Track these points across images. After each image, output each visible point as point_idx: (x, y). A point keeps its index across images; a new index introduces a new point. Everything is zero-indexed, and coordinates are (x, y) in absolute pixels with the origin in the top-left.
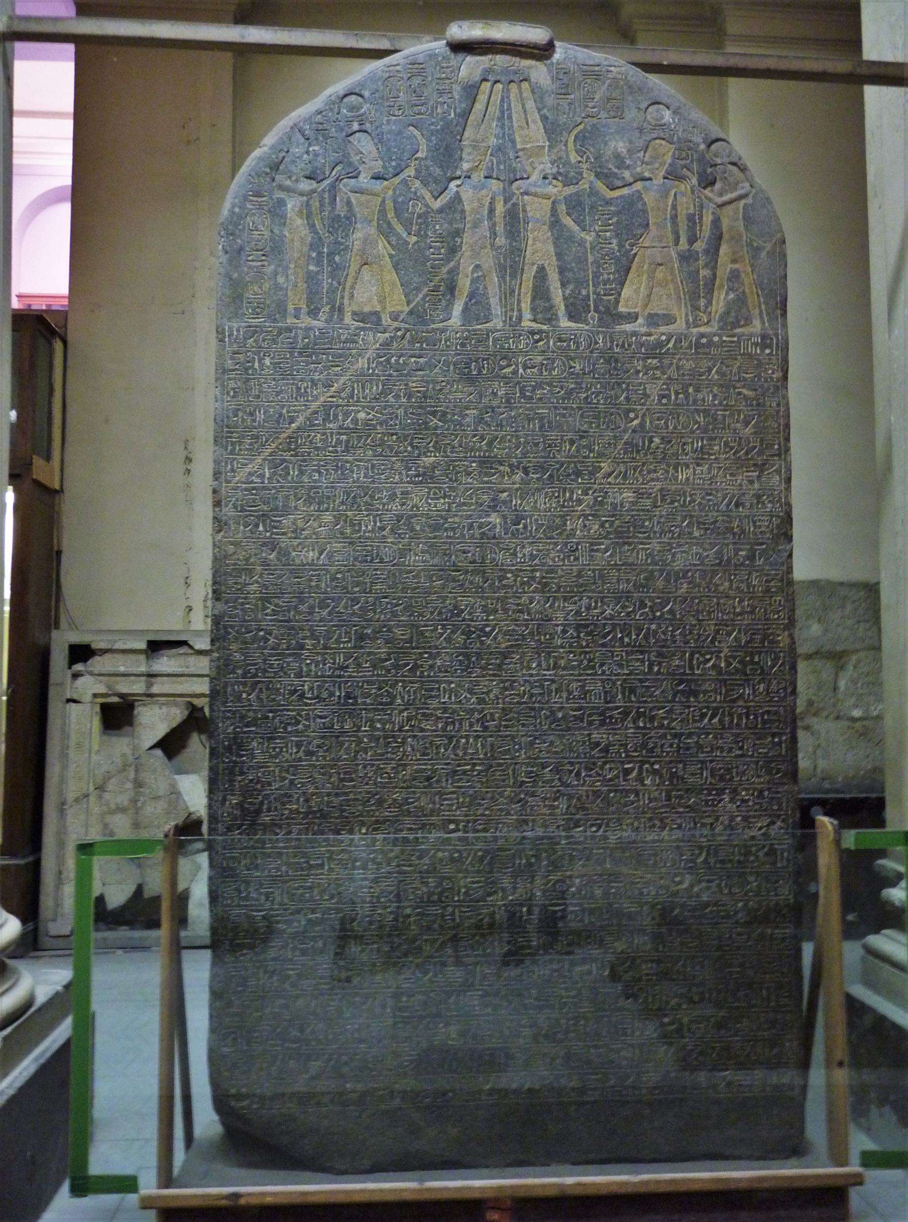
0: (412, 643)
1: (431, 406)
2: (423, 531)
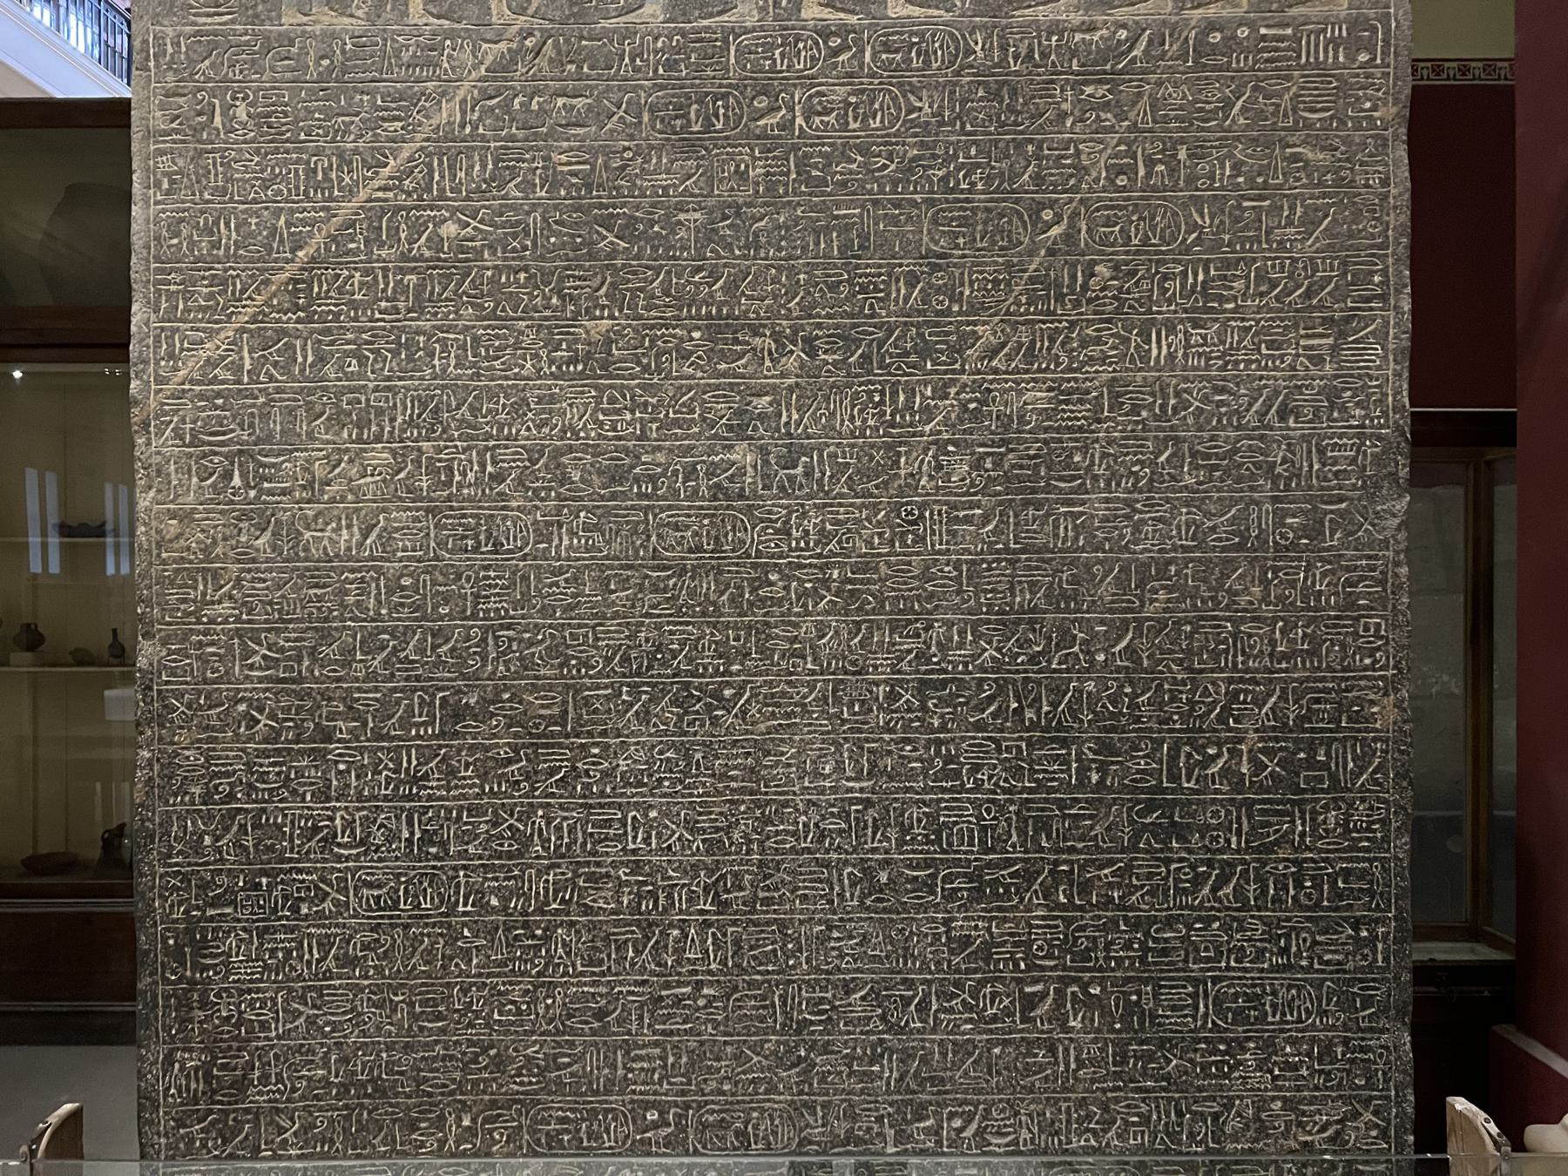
0: (564, 726)
1: (601, 206)
2: (590, 484)
